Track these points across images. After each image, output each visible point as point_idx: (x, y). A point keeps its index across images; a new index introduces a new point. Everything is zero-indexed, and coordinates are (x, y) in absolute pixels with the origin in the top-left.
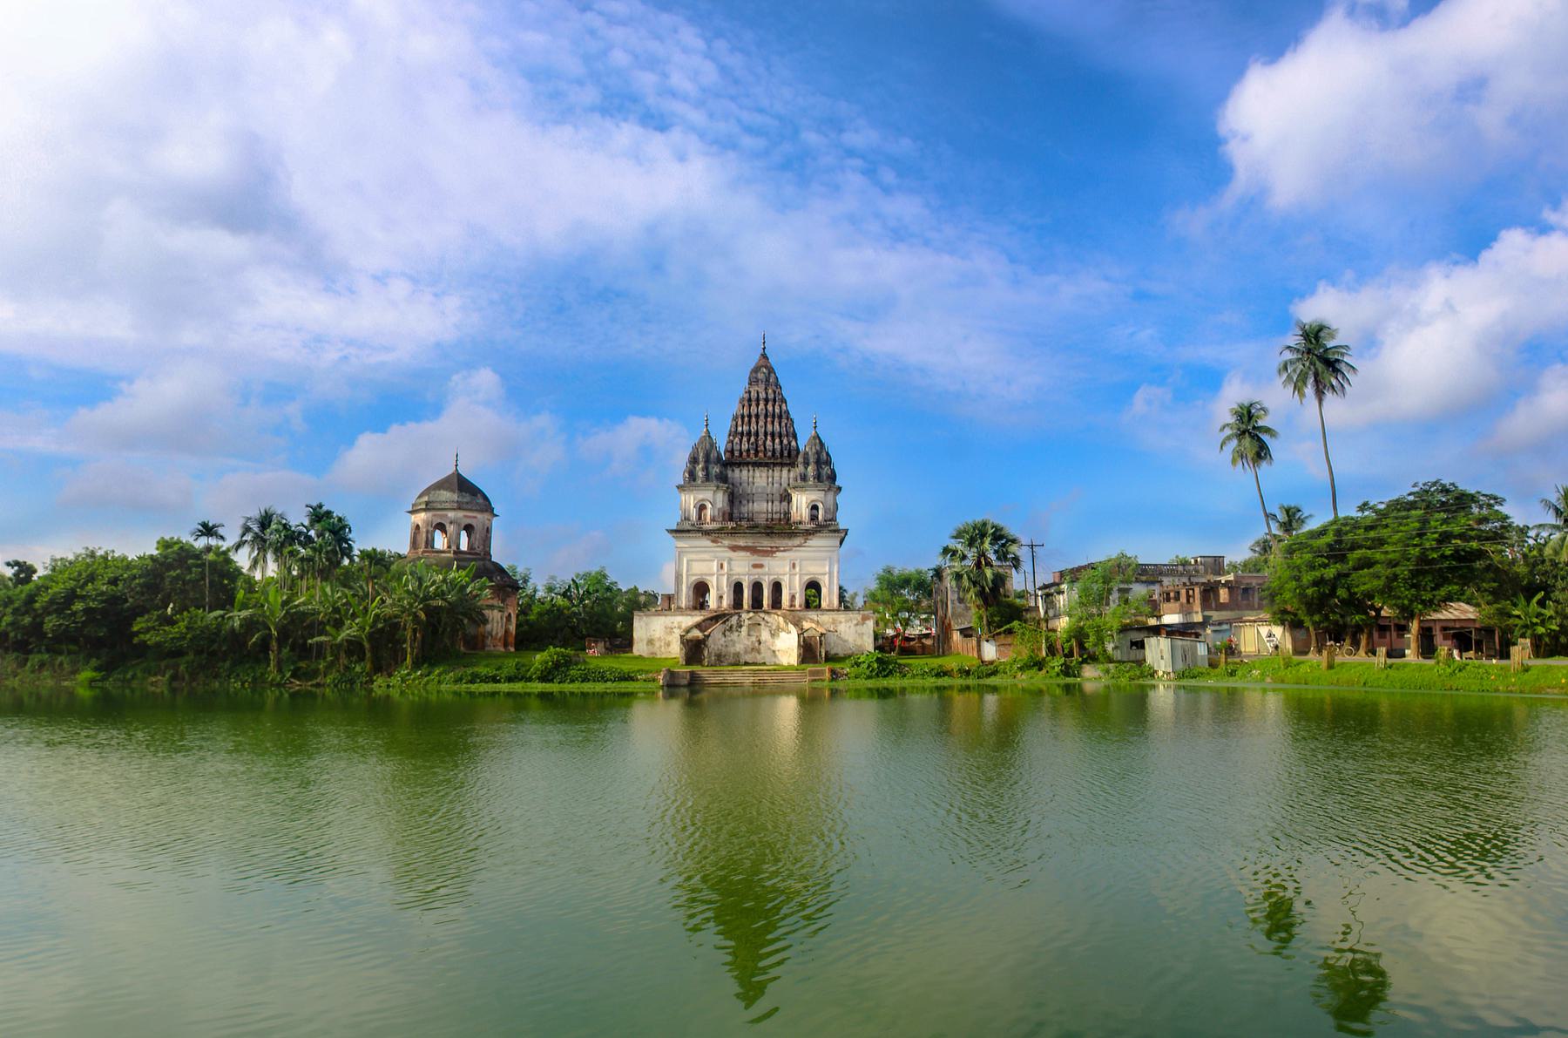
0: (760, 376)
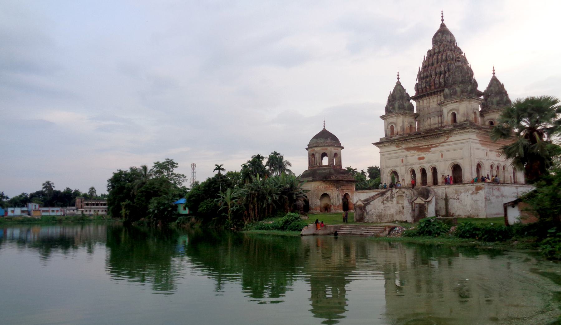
0: (437, 38)
